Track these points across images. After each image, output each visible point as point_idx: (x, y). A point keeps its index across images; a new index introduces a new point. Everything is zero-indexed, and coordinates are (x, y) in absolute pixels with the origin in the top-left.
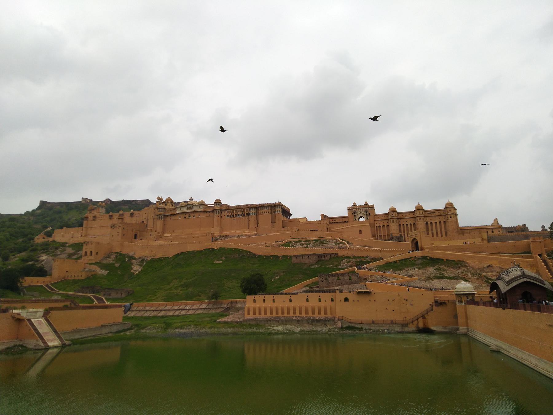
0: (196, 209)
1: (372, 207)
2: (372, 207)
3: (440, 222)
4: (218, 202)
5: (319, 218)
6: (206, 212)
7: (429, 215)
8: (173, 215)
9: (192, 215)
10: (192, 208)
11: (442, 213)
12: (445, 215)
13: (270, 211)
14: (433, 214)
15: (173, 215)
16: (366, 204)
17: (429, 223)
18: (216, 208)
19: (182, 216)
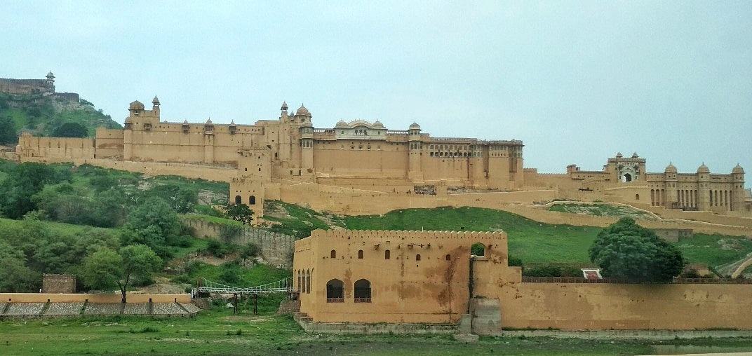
0: (372, 135)
1: (642, 162)
2: (642, 162)
3: (721, 191)
4: (415, 129)
5: (564, 171)
6: (392, 143)
7: (714, 180)
8: (330, 142)
9: (365, 147)
10: (366, 134)
11: (729, 179)
12: (733, 183)
13: (507, 153)
14: (718, 180)
15: (330, 142)
16: (635, 156)
17: (713, 191)
18: (414, 138)
19: (347, 147)
